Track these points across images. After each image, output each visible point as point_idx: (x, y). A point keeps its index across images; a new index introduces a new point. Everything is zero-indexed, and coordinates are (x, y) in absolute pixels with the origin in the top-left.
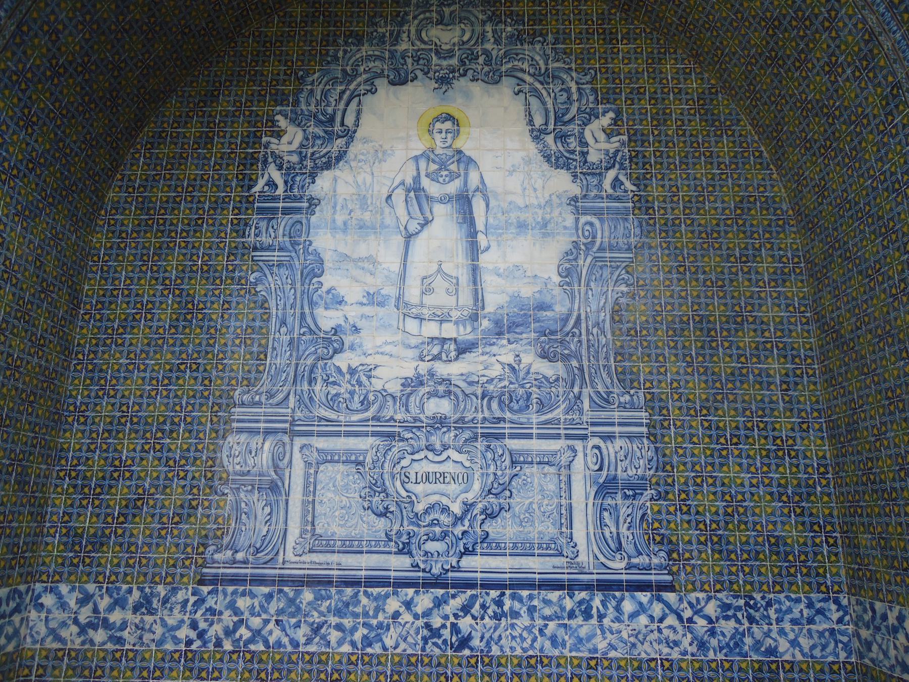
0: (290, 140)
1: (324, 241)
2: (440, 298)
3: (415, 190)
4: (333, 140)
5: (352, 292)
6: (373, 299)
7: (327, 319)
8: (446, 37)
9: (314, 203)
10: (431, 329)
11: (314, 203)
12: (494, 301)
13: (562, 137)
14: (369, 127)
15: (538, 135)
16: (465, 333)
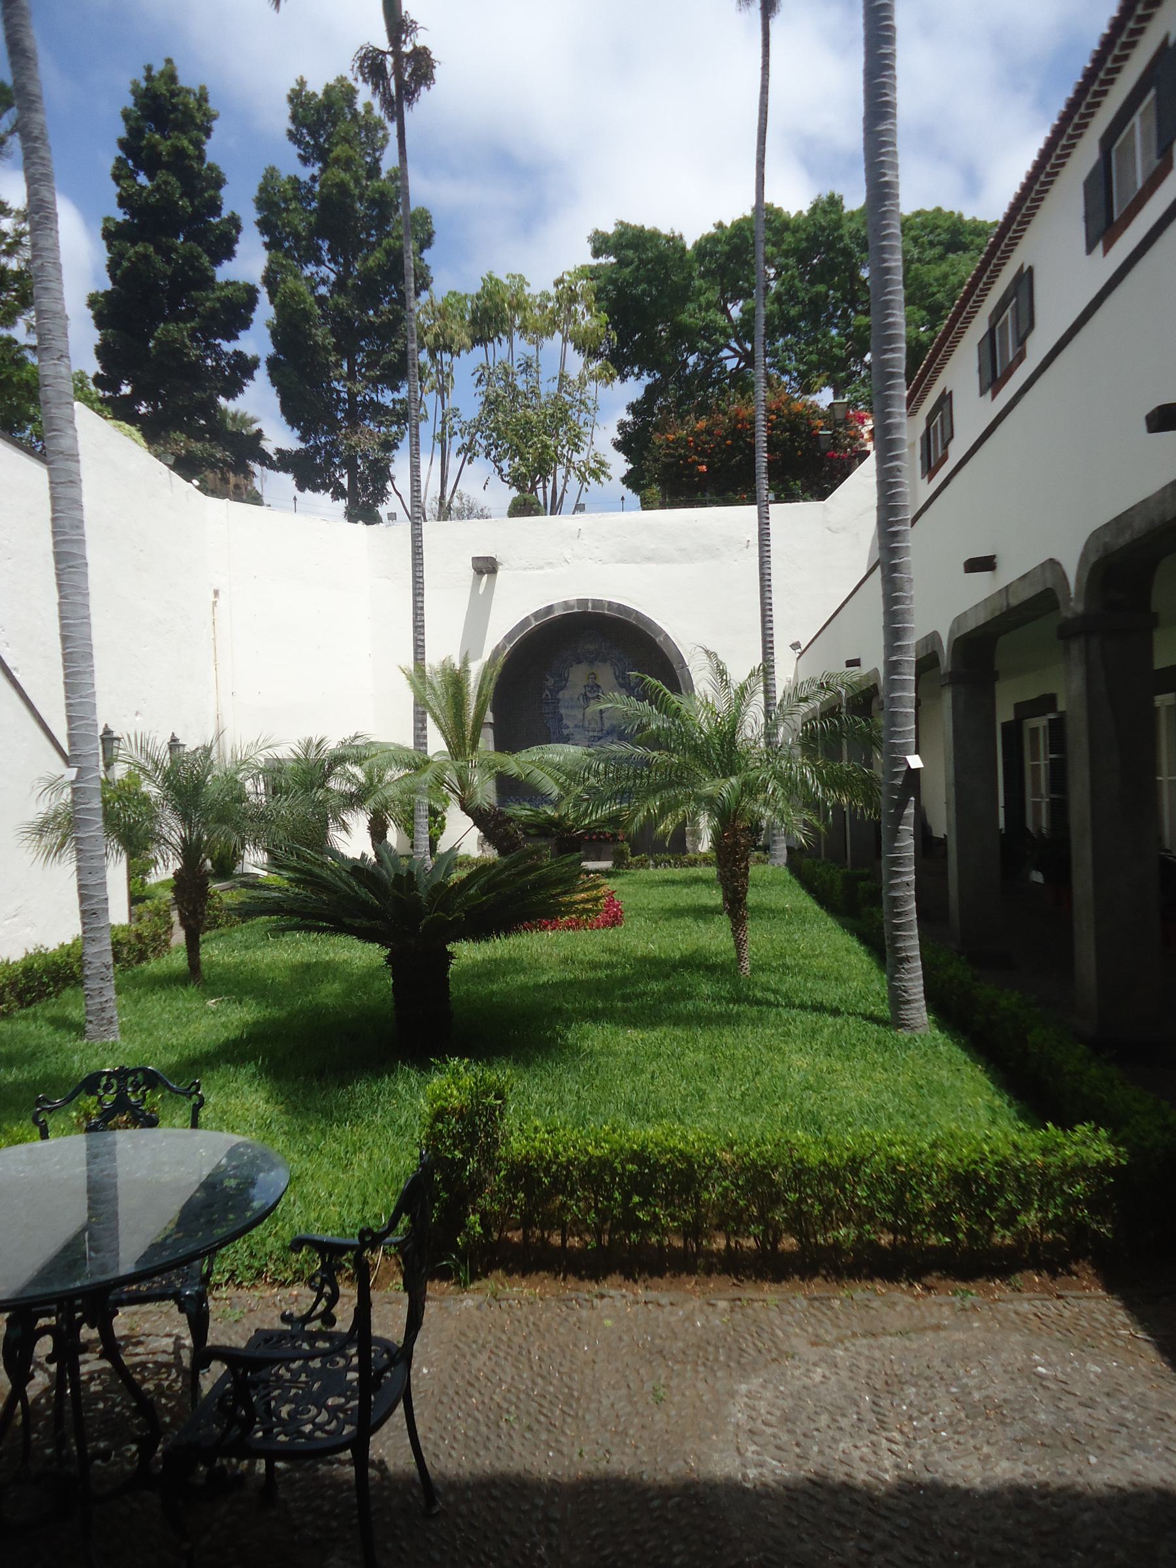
0: (550, 682)
1: (563, 711)
2: (593, 725)
3: (585, 695)
4: (562, 682)
5: (571, 724)
6: (576, 726)
7: (565, 732)
8: (591, 647)
9: (559, 700)
10: (591, 734)
11: (559, 700)
12: (607, 725)
13: (624, 678)
14: (571, 677)
15: (617, 678)
16: (600, 734)
